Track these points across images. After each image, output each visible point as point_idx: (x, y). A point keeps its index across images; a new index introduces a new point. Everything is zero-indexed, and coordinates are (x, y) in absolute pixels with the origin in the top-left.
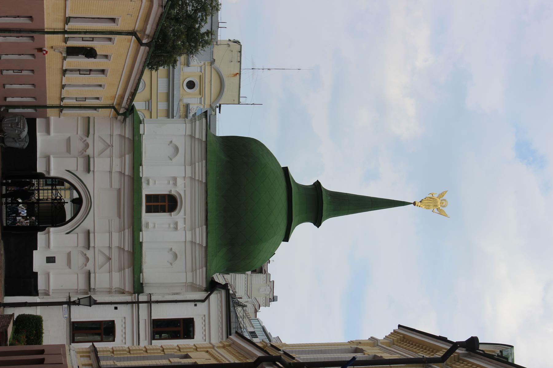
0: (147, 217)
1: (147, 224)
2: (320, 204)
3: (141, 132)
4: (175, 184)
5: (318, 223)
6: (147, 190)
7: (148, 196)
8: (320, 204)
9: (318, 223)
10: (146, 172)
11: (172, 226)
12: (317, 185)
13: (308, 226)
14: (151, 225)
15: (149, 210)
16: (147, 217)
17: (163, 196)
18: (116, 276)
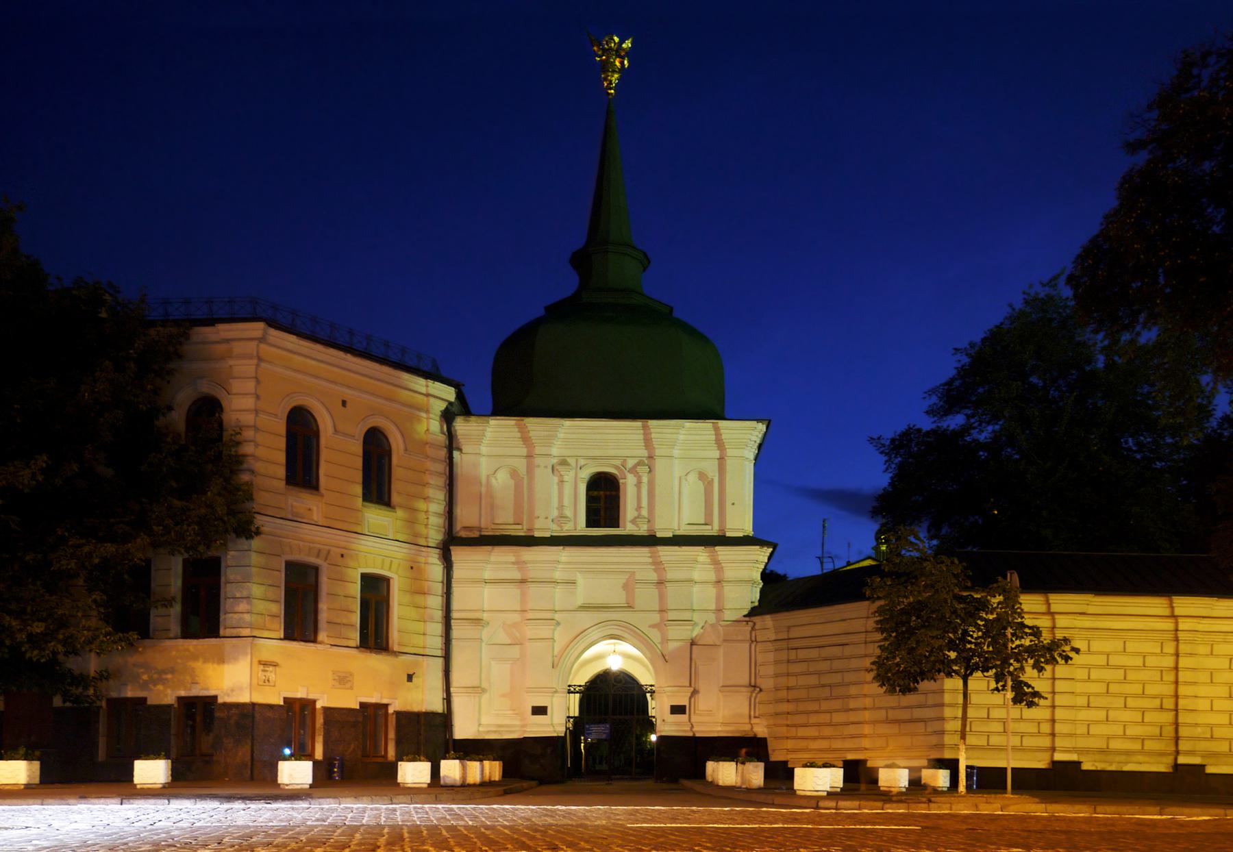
6: (578, 524)
7: (590, 523)
15: (615, 523)
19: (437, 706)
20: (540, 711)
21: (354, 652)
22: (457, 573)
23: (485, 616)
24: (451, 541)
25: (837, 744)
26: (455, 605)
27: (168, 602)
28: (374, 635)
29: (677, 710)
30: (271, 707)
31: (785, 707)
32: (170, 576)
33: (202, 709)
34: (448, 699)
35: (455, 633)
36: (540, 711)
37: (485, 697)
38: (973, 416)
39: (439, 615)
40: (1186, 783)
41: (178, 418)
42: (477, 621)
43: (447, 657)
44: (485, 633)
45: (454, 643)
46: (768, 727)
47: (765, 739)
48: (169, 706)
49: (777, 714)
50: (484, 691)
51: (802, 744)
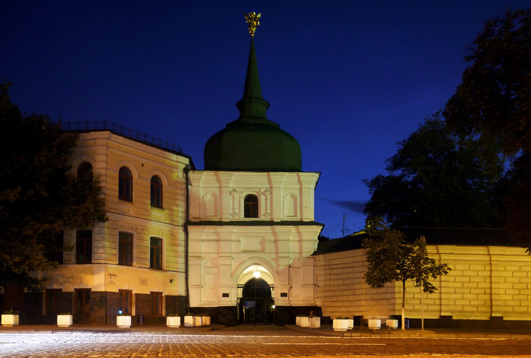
0: (262, 217)
6: (241, 216)
7: (246, 216)
15: (256, 216)
16: (262, 217)
19: (183, 293)
20: (226, 295)
21: (148, 270)
22: (191, 237)
23: (202, 255)
24: (188, 223)
25: (351, 309)
26: (190, 250)
27: (70, 249)
28: (156, 263)
29: (284, 295)
30: (113, 293)
31: (329, 294)
32: (71, 238)
33: (85, 295)
34: (187, 290)
35: (190, 262)
36: (226, 295)
37: (203, 289)
38: (405, 171)
39: (183, 254)
40: (495, 325)
41: (74, 171)
42: (199, 257)
43: (187, 273)
44: (202, 262)
45: (190, 267)
46: (322, 302)
47: (321, 307)
48: (71, 293)
49: (325, 297)
50: (202, 287)
51: (336, 309)
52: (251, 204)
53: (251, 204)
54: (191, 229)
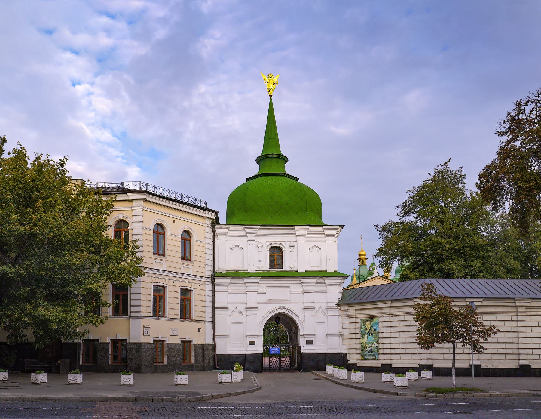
0: (286, 267)
1: (291, 267)
2: (271, 157)
3: (224, 272)
4: (262, 246)
5: (285, 159)
6: (266, 267)
7: (272, 266)
8: (271, 157)
9: (285, 159)
10: (252, 268)
11: (292, 250)
12: (259, 160)
13: (287, 165)
14: (293, 264)
16: (286, 267)
17: (270, 256)
18: (330, 288)
19: (211, 342)
20: (252, 343)
22: (217, 288)
27: (106, 304)
28: (185, 314)
35: (216, 312)
38: (417, 217)
40: (525, 371)
41: (110, 233)
42: (227, 308)
47: (346, 354)
52: (276, 254)
53: (276, 254)
54: (217, 280)
